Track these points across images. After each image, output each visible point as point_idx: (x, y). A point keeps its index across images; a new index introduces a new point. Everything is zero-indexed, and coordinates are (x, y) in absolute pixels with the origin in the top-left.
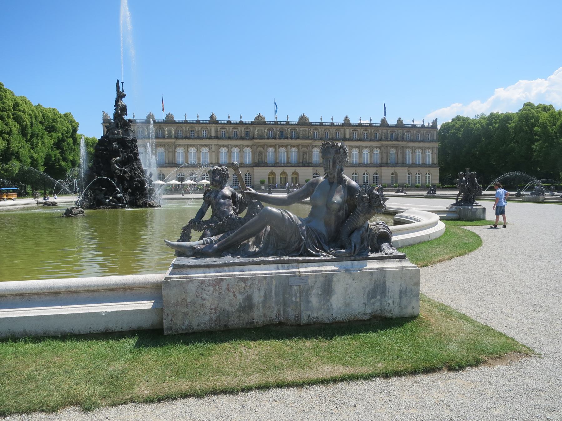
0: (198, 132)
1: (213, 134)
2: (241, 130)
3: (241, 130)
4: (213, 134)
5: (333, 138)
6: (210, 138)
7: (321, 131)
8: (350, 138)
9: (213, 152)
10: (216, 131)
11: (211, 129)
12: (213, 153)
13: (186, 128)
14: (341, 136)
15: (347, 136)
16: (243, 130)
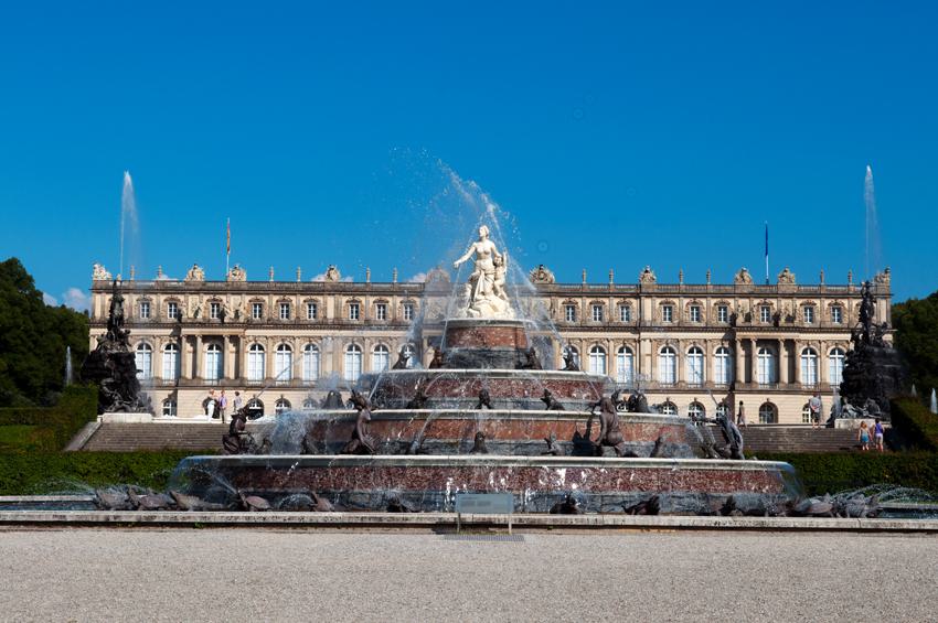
0: (297, 307)
1: (331, 315)
2: (394, 305)
3: (394, 305)
4: (331, 315)
5: (611, 320)
6: (323, 325)
7: (583, 304)
8: (654, 320)
9: (330, 353)
10: (337, 307)
11: (326, 303)
12: (330, 357)
13: (270, 300)
14: (634, 317)
15: (648, 316)
16: (398, 304)
